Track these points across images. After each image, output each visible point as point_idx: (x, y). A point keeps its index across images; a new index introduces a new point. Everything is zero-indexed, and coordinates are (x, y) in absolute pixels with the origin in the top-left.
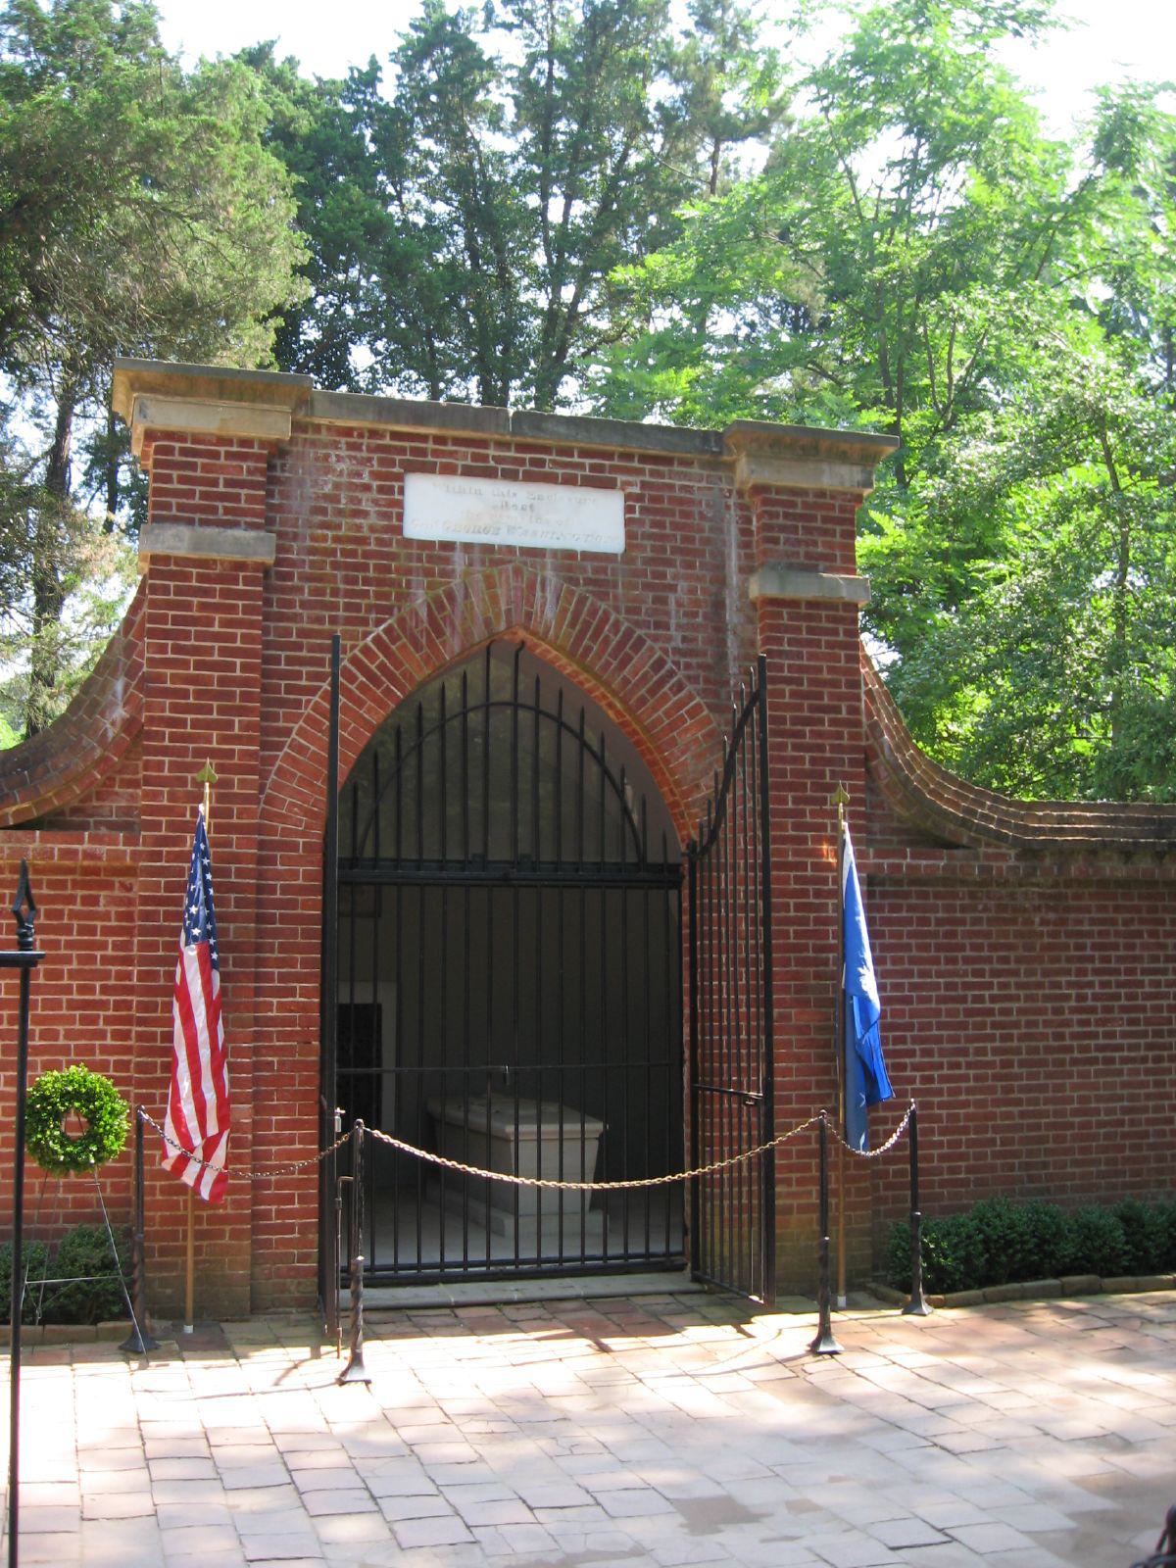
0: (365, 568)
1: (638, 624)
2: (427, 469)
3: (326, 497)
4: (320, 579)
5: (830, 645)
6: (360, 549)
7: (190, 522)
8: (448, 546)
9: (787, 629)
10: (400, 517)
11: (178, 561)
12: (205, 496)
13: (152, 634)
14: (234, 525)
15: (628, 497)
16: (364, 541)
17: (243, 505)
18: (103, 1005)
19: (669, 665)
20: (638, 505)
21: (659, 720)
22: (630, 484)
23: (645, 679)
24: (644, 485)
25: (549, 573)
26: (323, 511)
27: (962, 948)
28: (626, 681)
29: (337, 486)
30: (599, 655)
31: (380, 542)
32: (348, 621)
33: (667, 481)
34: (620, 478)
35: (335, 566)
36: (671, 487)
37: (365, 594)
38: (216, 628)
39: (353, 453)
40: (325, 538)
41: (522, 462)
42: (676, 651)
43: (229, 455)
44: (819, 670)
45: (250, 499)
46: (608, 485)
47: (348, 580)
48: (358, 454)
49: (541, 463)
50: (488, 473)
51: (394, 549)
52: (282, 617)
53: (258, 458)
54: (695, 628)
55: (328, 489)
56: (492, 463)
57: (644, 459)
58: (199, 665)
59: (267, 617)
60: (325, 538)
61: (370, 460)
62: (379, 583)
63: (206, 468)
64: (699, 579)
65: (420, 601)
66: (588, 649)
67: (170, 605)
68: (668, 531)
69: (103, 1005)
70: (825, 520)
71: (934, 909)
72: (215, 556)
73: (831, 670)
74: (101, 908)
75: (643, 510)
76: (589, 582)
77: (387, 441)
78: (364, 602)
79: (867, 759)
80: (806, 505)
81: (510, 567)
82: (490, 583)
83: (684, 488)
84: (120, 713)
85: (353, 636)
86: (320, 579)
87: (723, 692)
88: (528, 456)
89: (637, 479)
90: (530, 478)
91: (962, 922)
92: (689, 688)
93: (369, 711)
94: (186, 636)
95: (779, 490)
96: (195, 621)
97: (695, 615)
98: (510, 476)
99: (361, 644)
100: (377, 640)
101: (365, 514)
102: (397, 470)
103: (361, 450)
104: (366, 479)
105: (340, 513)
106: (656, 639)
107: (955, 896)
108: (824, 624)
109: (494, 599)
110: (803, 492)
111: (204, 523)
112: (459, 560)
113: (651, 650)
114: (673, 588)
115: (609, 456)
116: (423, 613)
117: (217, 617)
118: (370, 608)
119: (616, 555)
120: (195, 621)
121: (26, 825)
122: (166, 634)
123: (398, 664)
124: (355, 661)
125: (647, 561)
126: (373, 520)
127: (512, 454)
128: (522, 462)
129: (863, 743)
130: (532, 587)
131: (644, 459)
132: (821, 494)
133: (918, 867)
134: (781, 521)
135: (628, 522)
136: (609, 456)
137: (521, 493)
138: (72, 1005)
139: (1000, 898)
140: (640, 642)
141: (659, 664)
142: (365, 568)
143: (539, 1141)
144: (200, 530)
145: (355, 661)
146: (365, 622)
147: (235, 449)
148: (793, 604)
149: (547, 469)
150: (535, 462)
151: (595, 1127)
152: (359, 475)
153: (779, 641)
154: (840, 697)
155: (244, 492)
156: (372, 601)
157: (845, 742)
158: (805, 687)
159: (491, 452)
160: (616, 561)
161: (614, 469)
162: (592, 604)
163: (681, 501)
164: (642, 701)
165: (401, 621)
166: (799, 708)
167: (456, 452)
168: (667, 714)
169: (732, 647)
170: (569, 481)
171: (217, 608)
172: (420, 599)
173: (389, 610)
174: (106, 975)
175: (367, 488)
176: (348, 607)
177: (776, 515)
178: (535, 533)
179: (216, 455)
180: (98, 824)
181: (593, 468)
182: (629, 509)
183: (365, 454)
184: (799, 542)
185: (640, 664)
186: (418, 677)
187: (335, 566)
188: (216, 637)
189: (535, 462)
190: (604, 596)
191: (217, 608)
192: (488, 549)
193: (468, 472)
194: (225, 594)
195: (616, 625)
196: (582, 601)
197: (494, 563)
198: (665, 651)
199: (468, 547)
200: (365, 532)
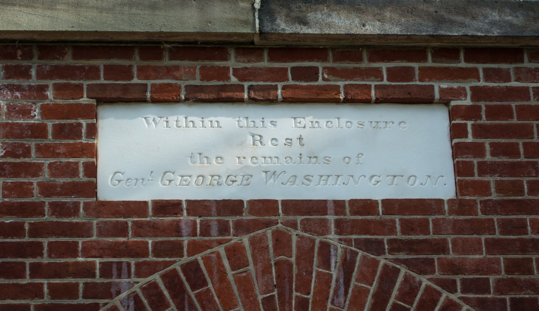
6: (27, 222)
15: (453, 114)
20: (469, 123)
22: (459, 93)
24: (477, 93)
25: (332, 238)
33: (514, 84)
36: (523, 93)
39: (15, 82)
41: (281, 75)
48: (25, 83)
51: (80, 219)
56: (234, 80)
61: (42, 89)
65: (124, 295)
68: (522, 159)
75: (479, 131)
81: (269, 232)
89: (467, 85)
102: (85, 100)
103: (29, 77)
104: (36, 117)
127: (265, 64)
149: (320, 82)
152: (26, 112)
160: (440, 211)
162: (407, 279)
167: (177, 68)
178: (308, 178)
183: (34, 81)
200: (36, 197)
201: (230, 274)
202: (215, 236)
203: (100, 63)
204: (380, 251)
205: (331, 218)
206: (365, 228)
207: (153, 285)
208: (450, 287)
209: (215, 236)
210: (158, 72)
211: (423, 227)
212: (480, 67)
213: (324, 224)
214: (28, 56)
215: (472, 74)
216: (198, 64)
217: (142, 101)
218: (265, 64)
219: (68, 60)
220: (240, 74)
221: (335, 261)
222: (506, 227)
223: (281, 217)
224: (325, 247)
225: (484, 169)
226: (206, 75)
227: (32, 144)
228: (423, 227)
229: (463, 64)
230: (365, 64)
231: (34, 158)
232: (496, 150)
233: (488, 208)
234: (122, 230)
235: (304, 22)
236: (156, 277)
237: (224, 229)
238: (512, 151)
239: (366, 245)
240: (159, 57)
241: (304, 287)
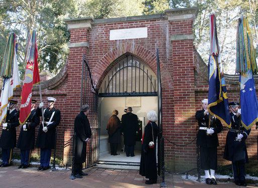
3: (97, 36)
5: (186, 48)
8: (116, 41)
10: (109, 37)
23: (150, 58)
44: (184, 53)
49: (132, 25)
52: (90, 55)
58: (76, 63)
62: (105, 48)
70: (185, 25)
76: (140, 43)
77: (107, 26)
82: (123, 46)
84: (65, 71)
87: (166, 59)
96: (75, 57)
105: (99, 38)
108: (185, 44)
109: (124, 48)
112: (118, 43)
114: (156, 42)
120: (75, 57)
121: (51, 89)
122: (72, 59)
125: (151, 38)
126: (104, 38)
129: (193, 66)
130: (130, 45)
132: (184, 21)
141: (153, 55)
148: (178, 41)
163: (157, 27)
164: (150, 62)
165: (108, 54)
166: (180, 60)
169: (167, 51)
171: (79, 55)
172: (111, 50)
173: (106, 52)
175: (103, 33)
182: (148, 30)
185: (149, 56)
186: (111, 62)
188: (79, 59)
190: (143, 45)
191: (79, 55)
193: (120, 28)
222: (153, 40)
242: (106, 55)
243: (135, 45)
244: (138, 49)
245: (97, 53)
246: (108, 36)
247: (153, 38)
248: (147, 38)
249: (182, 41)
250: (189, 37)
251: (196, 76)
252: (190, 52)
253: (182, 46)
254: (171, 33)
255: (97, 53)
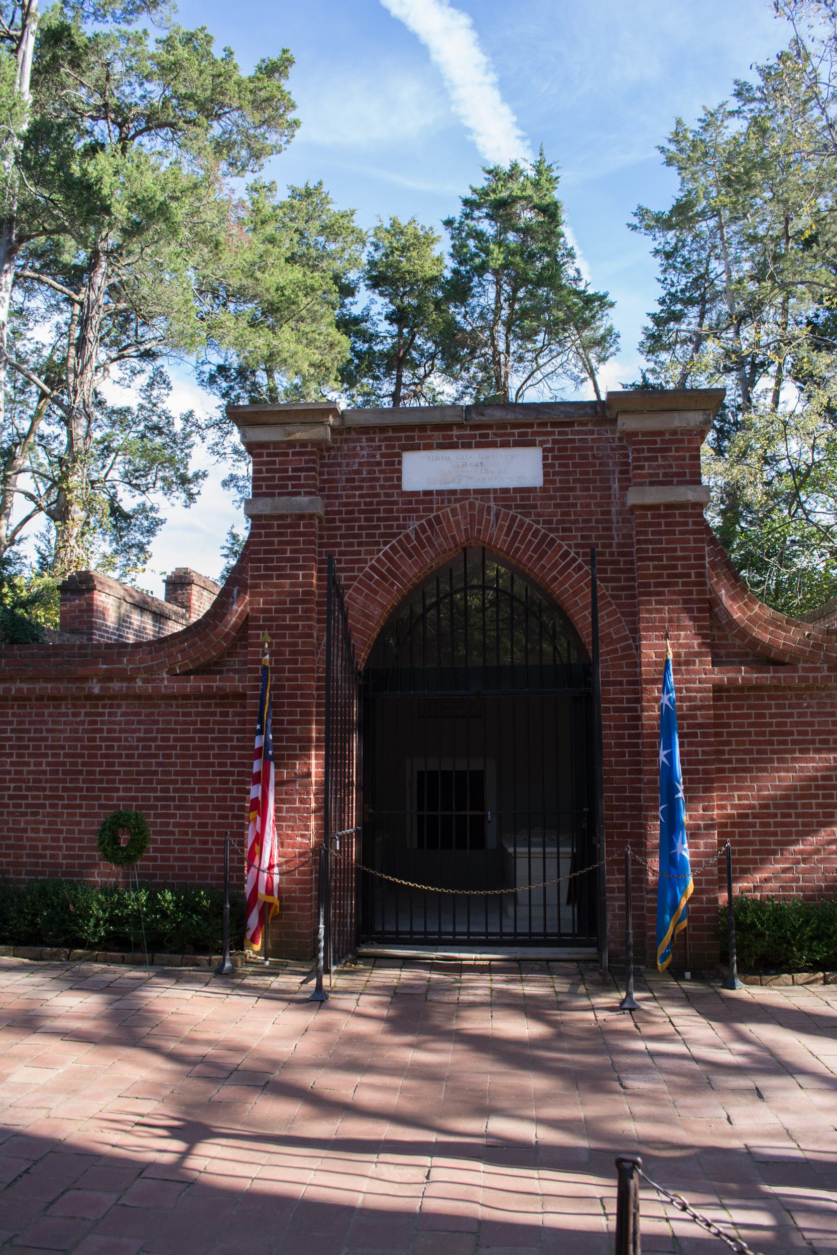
0: (378, 511)
1: (551, 530)
2: (415, 448)
4: (352, 520)
5: (682, 533)
7: (273, 495)
8: (428, 493)
9: (650, 525)
10: (399, 479)
11: (267, 517)
12: (281, 479)
13: (252, 561)
14: (298, 494)
15: (544, 450)
16: (378, 495)
17: (302, 482)
18: (231, 773)
19: (573, 554)
21: (566, 590)
22: (546, 442)
23: (556, 564)
25: (492, 504)
26: (353, 480)
27: (791, 733)
28: (543, 567)
29: (360, 464)
30: (525, 553)
31: (387, 495)
32: (367, 544)
34: (538, 439)
35: (360, 512)
36: (572, 441)
37: (378, 527)
38: (288, 555)
40: (354, 496)
41: (474, 436)
42: (577, 546)
43: (294, 454)
44: (675, 550)
45: (306, 478)
46: (531, 444)
47: (366, 520)
49: (487, 436)
50: (453, 446)
53: (311, 453)
54: (591, 529)
55: (356, 467)
57: (554, 424)
59: (321, 545)
60: (354, 496)
63: (281, 463)
64: (593, 497)
66: (518, 549)
67: (262, 543)
69: (231, 773)
71: (769, 707)
72: (285, 512)
73: (683, 549)
74: (230, 719)
75: (554, 458)
76: (517, 507)
78: (377, 532)
79: (711, 609)
80: (663, 442)
83: (580, 440)
85: (370, 553)
86: (352, 520)
88: (478, 432)
89: (550, 438)
90: (479, 445)
91: (790, 715)
92: (586, 568)
93: (381, 597)
94: (271, 560)
95: (644, 434)
97: (590, 521)
98: (467, 446)
99: (376, 557)
100: (386, 554)
101: (377, 479)
104: (378, 458)
106: (563, 539)
107: (784, 698)
110: (660, 433)
111: (280, 494)
113: (560, 546)
115: (531, 425)
116: (413, 537)
117: (289, 548)
118: (382, 535)
119: (535, 488)
121: (187, 673)
122: (260, 560)
123: (398, 567)
124: (373, 568)
127: (468, 432)
128: (474, 436)
131: (554, 424)
132: (674, 432)
133: (750, 679)
134: (646, 454)
135: (545, 466)
136: (531, 425)
137: (473, 456)
138: (216, 773)
139: (821, 698)
140: (553, 541)
141: (567, 554)
142: (378, 511)
143: (530, 858)
144: (277, 498)
145: (373, 568)
146: (378, 544)
147: (297, 450)
150: (482, 436)
151: (566, 850)
152: (374, 456)
153: (645, 533)
154: (690, 567)
155: (303, 474)
156: (382, 531)
157: (694, 597)
158: (665, 562)
159: (455, 432)
161: (535, 434)
166: (660, 576)
168: (571, 586)
170: (505, 445)
171: (288, 543)
173: (394, 535)
174: (233, 756)
175: (379, 464)
176: (368, 536)
177: (643, 451)
179: (287, 455)
180: (228, 671)
181: (520, 435)
182: (545, 458)
183: (377, 443)
184: (659, 467)
187: (360, 512)
189: (482, 436)
190: (527, 515)
191: (288, 543)
192: (453, 492)
193: (442, 446)
194: (294, 534)
195: (537, 531)
196: (514, 518)
197: (456, 501)
198: (569, 546)
199: (440, 493)
200: (378, 491)
201: (452, 519)
202: (446, 504)
203: (403, 435)
204: (510, 509)
205: (492, 496)
206: (505, 499)
207: (422, 524)
208: (538, 522)
209: (446, 504)
210: (425, 438)
211: (528, 498)
212: (556, 430)
213: (489, 498)
214: (375, 433)
215: (553, 433)
216: (441, 433)
217: (419, 449)
218: (468, 432)
219: (390, 434)
220: (458, 437)
221: (493, 513)
222: (562, 498)
223: (472, 496)
224: (489, 507)
225: (555, 474)
226: (444, 437)
227: (376, 469)
228: (528, 498)
229: (549, 429)
230: (509, 431)
231: (377, 475)
232: (560, 465)
233: (555, 490)
234: (410, 503)
235: (482, 415)
236: (423, 521)
237: (450, 501)
238: (566, 466)
239: (505, 507)
240: (426, 431)
241: (480, 523)
242: (393, 548)
243: (497, 515)
244: (510, 528)
245: (354, 536)
246: (395, 470)
247: (561, 489)
248: (543, 489)
249: (669, 506)
250: (688, 494)
251: (716, 633)
252: (695, 549)
253: (667, 524)
254: (626, 472)
255: (354, 536)
